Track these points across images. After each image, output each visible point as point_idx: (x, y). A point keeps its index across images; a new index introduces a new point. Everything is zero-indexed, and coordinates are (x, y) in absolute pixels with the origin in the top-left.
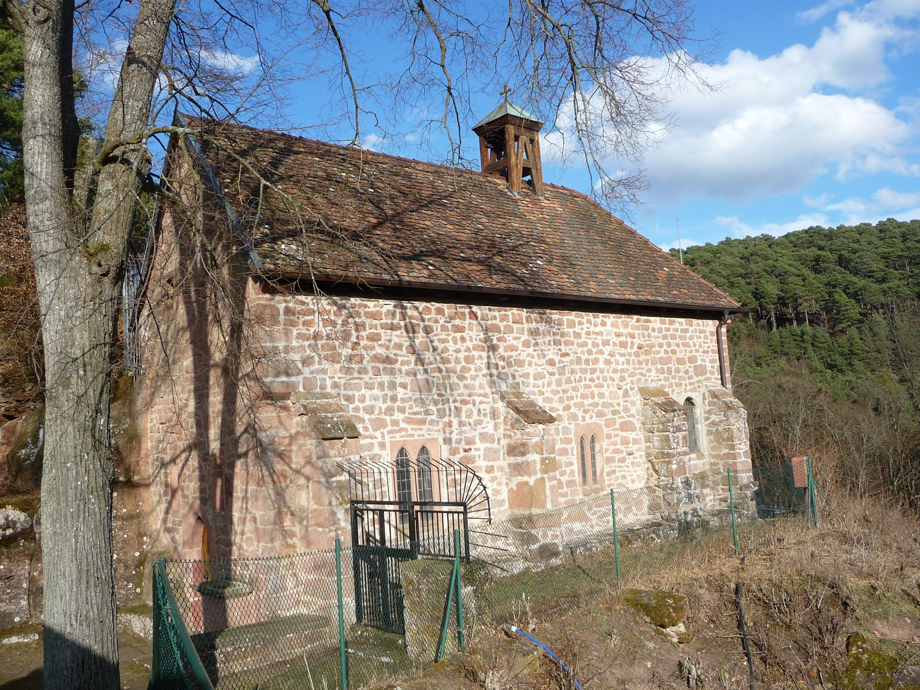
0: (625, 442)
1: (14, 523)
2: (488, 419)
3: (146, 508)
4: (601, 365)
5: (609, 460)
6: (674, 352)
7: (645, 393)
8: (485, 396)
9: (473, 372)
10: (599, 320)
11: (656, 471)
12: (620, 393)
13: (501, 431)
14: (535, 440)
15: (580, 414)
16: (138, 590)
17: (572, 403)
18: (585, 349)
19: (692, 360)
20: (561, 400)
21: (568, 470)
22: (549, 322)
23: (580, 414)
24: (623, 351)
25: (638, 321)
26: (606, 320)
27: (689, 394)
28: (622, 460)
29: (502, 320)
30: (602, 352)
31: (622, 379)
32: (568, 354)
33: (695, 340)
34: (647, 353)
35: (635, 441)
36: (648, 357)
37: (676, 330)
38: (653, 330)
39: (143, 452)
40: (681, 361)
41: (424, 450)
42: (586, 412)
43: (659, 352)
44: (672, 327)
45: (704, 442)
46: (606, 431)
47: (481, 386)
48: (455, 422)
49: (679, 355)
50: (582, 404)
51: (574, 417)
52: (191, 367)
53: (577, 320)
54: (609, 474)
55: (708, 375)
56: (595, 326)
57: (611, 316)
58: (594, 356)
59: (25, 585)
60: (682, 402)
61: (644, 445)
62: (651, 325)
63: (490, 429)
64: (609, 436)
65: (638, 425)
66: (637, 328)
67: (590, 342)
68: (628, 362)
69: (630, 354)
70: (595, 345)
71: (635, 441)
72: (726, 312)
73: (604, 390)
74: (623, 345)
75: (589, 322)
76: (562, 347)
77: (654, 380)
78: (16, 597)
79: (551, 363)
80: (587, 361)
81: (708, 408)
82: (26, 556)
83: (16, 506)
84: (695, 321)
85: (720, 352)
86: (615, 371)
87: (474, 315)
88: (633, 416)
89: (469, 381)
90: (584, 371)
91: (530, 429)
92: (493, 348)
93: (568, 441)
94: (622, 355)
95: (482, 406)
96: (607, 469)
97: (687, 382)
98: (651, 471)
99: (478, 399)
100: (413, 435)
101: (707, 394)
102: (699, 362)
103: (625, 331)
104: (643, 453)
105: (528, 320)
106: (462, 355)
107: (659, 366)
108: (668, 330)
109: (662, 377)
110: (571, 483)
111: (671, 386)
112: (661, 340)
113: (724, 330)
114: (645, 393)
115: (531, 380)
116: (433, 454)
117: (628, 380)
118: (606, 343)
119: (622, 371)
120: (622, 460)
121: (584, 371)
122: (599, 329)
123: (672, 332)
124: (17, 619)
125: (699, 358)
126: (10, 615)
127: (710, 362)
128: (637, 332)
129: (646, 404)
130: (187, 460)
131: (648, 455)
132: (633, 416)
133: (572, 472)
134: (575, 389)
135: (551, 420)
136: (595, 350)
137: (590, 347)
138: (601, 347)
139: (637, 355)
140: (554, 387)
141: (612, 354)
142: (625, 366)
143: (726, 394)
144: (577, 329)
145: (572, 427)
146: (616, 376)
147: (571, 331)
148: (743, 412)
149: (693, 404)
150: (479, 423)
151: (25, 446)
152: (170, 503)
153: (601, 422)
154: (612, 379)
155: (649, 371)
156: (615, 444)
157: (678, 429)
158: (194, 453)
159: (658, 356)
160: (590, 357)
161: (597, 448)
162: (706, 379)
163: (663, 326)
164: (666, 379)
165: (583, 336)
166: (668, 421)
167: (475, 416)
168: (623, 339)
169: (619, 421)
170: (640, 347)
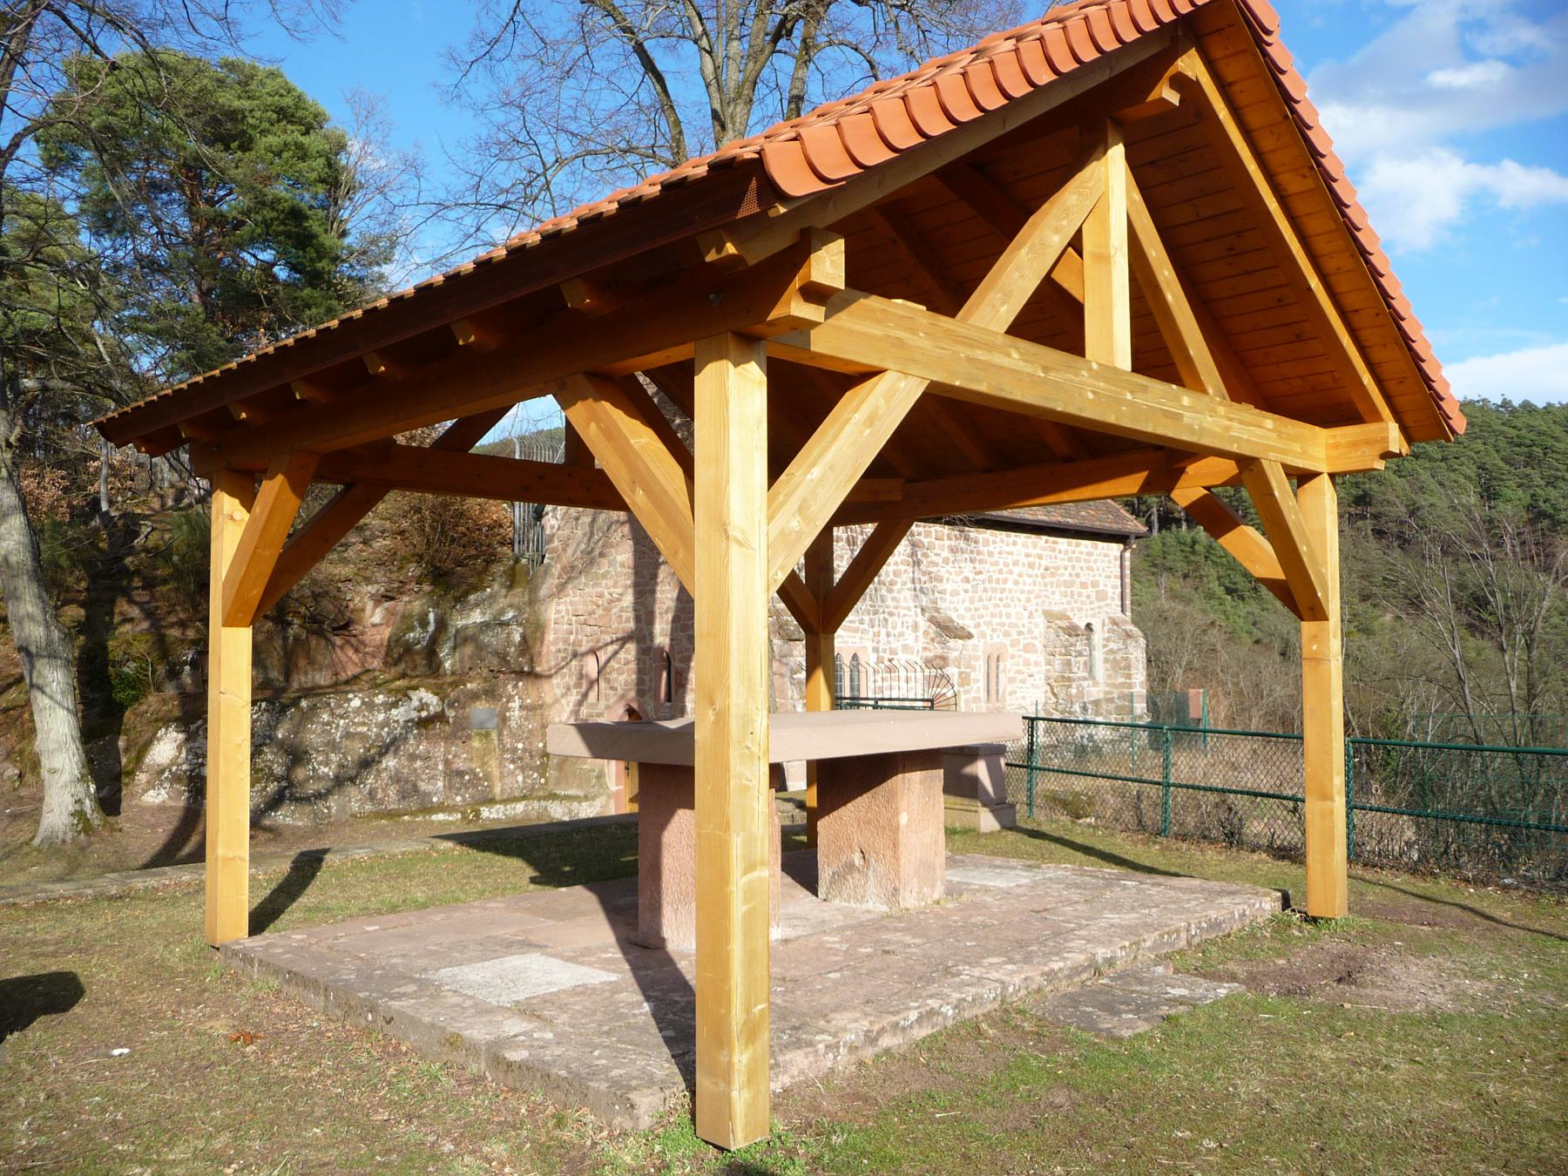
0: (1027, 663)
1: (428, 705)
2: (910, 631)
3: (548, 699)
4: (1010, 585)
5: (1012, 680)
6: (1078, 575)
7: (1049, 616)
8: (909, 609)
11: (1054, 694)
12: (1026, 614)
13: (921, 645)
14: (955, 654)
15: (989, 632)
16: (543, 781)
17: (982, 621)
18: (997, 568)
19: (1095, 584)
20: (973, 618)
22: (967, 539)
23: (989, 632)
24: (1030, 572)
25: (1047, 542)
26: (1017, 539)
27: (1089, 620)
28: (1023, 681)
29: (926, 536)
30: (1011, 572)
31: (1028, 600)
33: (1099, 564)
34: (1053, 575)
35: (1036, 664)
36: (1054, 580)
37: (1081, 553)
38: (1060, 552)
39: (546, 642)
40: (1084, 585)
41: (855, 657)
42: (994, 630)
43: (1063, 575)
44: (1078, 549)
45: (1100, 670)
47: (905, 598)
48: (883, 631)
49: (1083, 579)
50: (990, 624)
51: (983, 635)
52: (631, 563)
53: (991, 539)
54: (1010, 694)
55: (1109, 601)
57: (1023, 535)
58: (1004, 575)
59: (440, 767)
60: (1083, 626)
61: (1044, 668)
63: (911, 642)
64: (1013, 657)
65: (1040, 647)
67: (1001, 561)
69: (1037, 576)
70: (1006, 565)
71: (1036, 664)
72: (1133, 537)
73: (1011, 610)
74: (1031, 566)
75: (1002, 541)
76: (977, 565)
77: (1057, 603)
78: (433, 777)
79: (967, 580)
80: (998, 580)
81: (1107, 635)
82: (442, 738)
83: (428, 689)
84: (1100, 544)
85: (1122, 577)
86: (1022, 592)
88: (1035, 638)
89: (895, 595)
90: (994, 590)
91: (952, 643)
92: (917, 563)
93: (977, 658)
94: (1030, 576)
95: (906, 619)
96: (1009, 689)
97: (1089, 606)
98: (1050, 694)
99: (902, 612)
100: (847, 642)
101: (1107, 621)
102: (1101, 587)
103: (1034, 552)
104: (1043, 676)
105: (949, 538)
107: (1063, 589)
108: (1074, 552)
109: (1064, 600)
110: (977, 699)
111: (1072, 610)
112: (1066, 563)
113: (1128, 554)
114: (1049, 616)
116: (862, 660)
118: (1016, 563)
119: (1029, 592)
120: (1023, 681)
121: (994, 590)
122: (1011, 549)
123: (1077, 555)
124: (435, 799)
126: (429, 795)
127: (1112, 587)
128: (1044, 553)
129: (1048, 627)
130: (616, 653)
131: (1048, 678)
132: (1035, 638)
133: (978, 690)
134: (986, 608)
135: (970, 636)
136: (1005, 569)
137: (1001, 566)
138: (1011, 567)
139: (1043, 576)
140: (967, 604)
141: (1020, 575)
142: (1031, 588)
143: (1124, 622)
144: (991, 548)
145: (981, 645)
146: (1023, 597)
147: (985, 549)
148: (1142, 642)
149: (1091, 630)
150: (901, 634)
151: (412, 629)
152: (585, 696)
153: (1007, 641)
154: (1020, 600)
155: (1053, 593)
156: (1018, 665)
157: (1080, 654)
158: (631, 647)
159: (1062, 579)
160: (1001, 577)
161: (1001, 668)
162: (1107, 605)
163: (1070, 548)
164: (1069, 603)
165: (996, 555)
166: (1072, 645)
167: (899, 628)
168: (1031, 559)
169: (1023, 642)
170: (1046, 569)
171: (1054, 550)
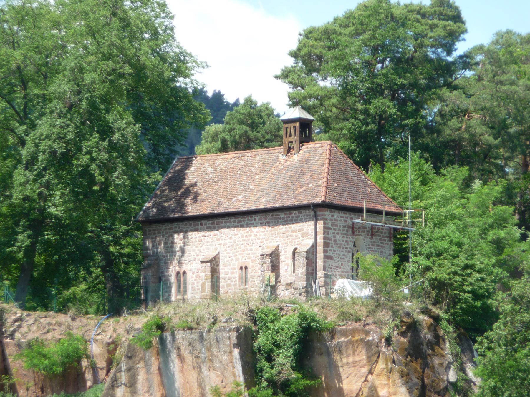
9: (201, 245)
10: (253, 218)
15: (241, 258)
17: (238, 254)
21: (234, 280)
23: (241, 258)
32: (238, 234)
37: (293, 217)
38: (280, 219)
44: (290, 216)
46: (251, 264)
51: (238, 259)
56: (251, 221)
57: (259, 215)
62: (279, 217)
66: (272, 219)
68: (265, 235)
75: (248, 220)
80: (246, 236)
86: (259, 239)
87: (202, 224)
102: (305, 231)
106: (197, 240)
109: (282, 239)
115: (222, 246)
117: (265, 242)
122: (253, 222)
125: (305, 229)
128: (271, 221)
145: (237, 263)
160: (247, 234)
163: (286, 216)
171: (277, 218)
